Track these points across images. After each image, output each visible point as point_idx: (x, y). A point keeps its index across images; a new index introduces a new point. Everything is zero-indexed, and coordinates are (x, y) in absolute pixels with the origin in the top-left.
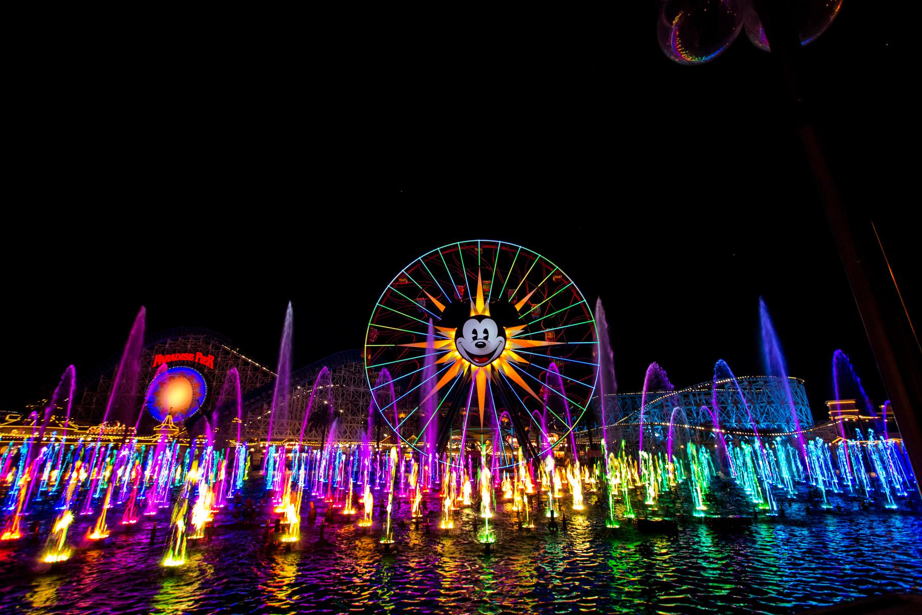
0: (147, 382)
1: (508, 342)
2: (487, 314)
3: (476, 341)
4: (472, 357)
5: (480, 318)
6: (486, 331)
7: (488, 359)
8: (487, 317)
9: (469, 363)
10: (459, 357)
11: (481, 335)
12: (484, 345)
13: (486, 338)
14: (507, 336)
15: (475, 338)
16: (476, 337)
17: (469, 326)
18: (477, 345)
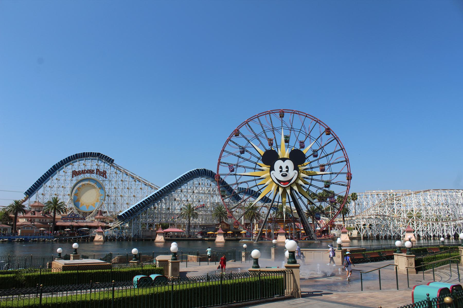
3: (282, 173)
5: (284, 160)
6: (287, 167)
7: (288, 183)
8: (286, 159)
11: (284, 169)
13: (287, 171)
15: (281, 171)
16: (282, 170)
17: (278, 164)
18: (282, 175)
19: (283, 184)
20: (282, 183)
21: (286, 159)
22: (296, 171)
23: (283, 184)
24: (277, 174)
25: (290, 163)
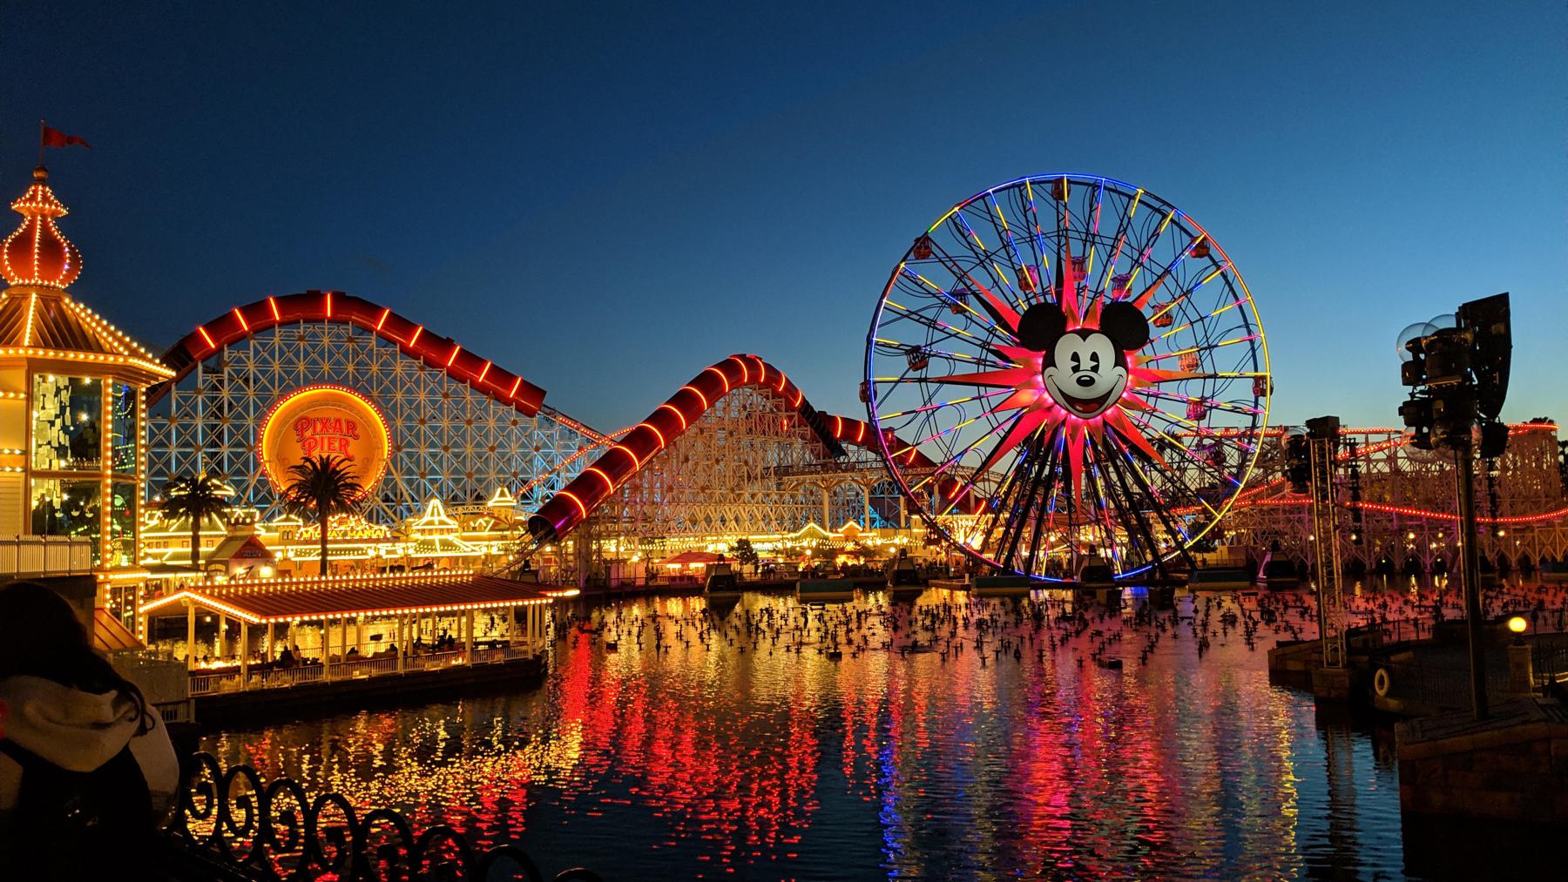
0: (250, 422)
1: (1130, 377)
2: (1096, 328)
3: (1079, 374)
4: (1071, 401)
5: (1084, 334)
6: (1094, 357)
9: (1064, 412)
10: (1050, 400)
11: (1086, 363)
12: (1091, 382)
13: (1095, 369)
14: (1130, 366)
15: (1076, 369)
16: (1078, 366)
17: (1066, 346)
18: (1079, 381)
19: (1081, 409)
20: (1078, 407)
21: (1093, 332)
22: (1120, 370)
23: (1081, 409)
24: (1063, 377)
25: (1102, 346)
